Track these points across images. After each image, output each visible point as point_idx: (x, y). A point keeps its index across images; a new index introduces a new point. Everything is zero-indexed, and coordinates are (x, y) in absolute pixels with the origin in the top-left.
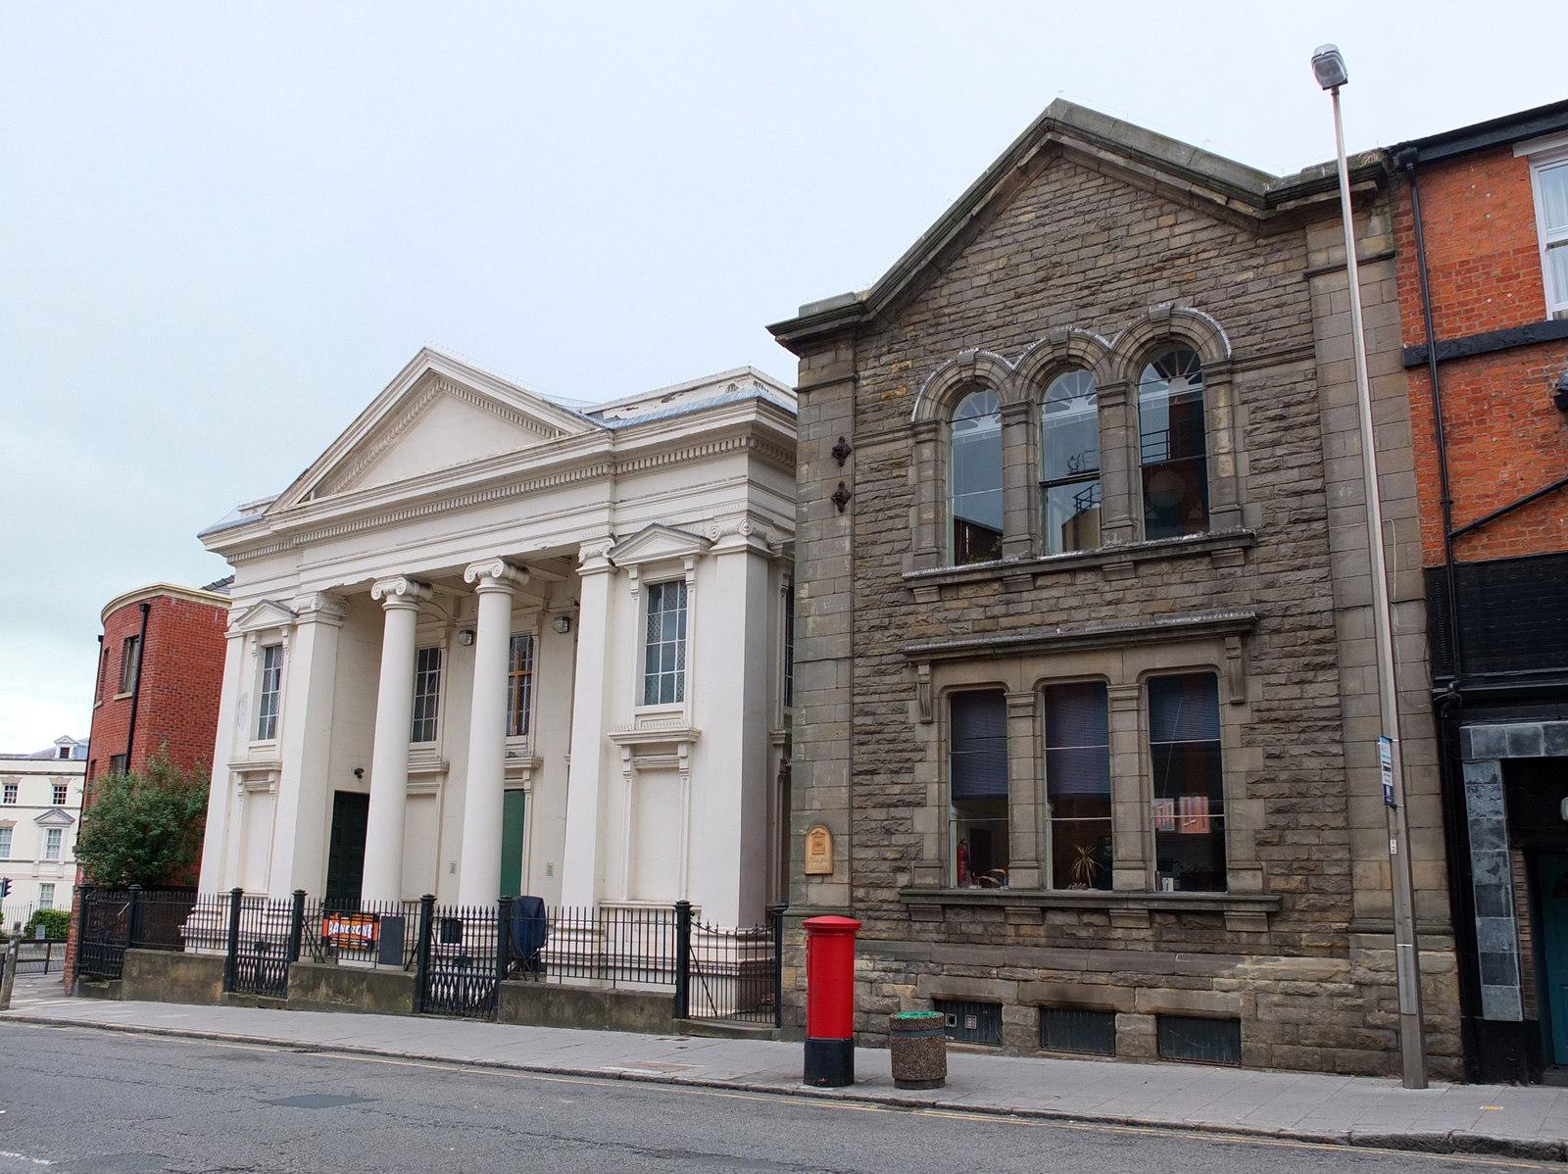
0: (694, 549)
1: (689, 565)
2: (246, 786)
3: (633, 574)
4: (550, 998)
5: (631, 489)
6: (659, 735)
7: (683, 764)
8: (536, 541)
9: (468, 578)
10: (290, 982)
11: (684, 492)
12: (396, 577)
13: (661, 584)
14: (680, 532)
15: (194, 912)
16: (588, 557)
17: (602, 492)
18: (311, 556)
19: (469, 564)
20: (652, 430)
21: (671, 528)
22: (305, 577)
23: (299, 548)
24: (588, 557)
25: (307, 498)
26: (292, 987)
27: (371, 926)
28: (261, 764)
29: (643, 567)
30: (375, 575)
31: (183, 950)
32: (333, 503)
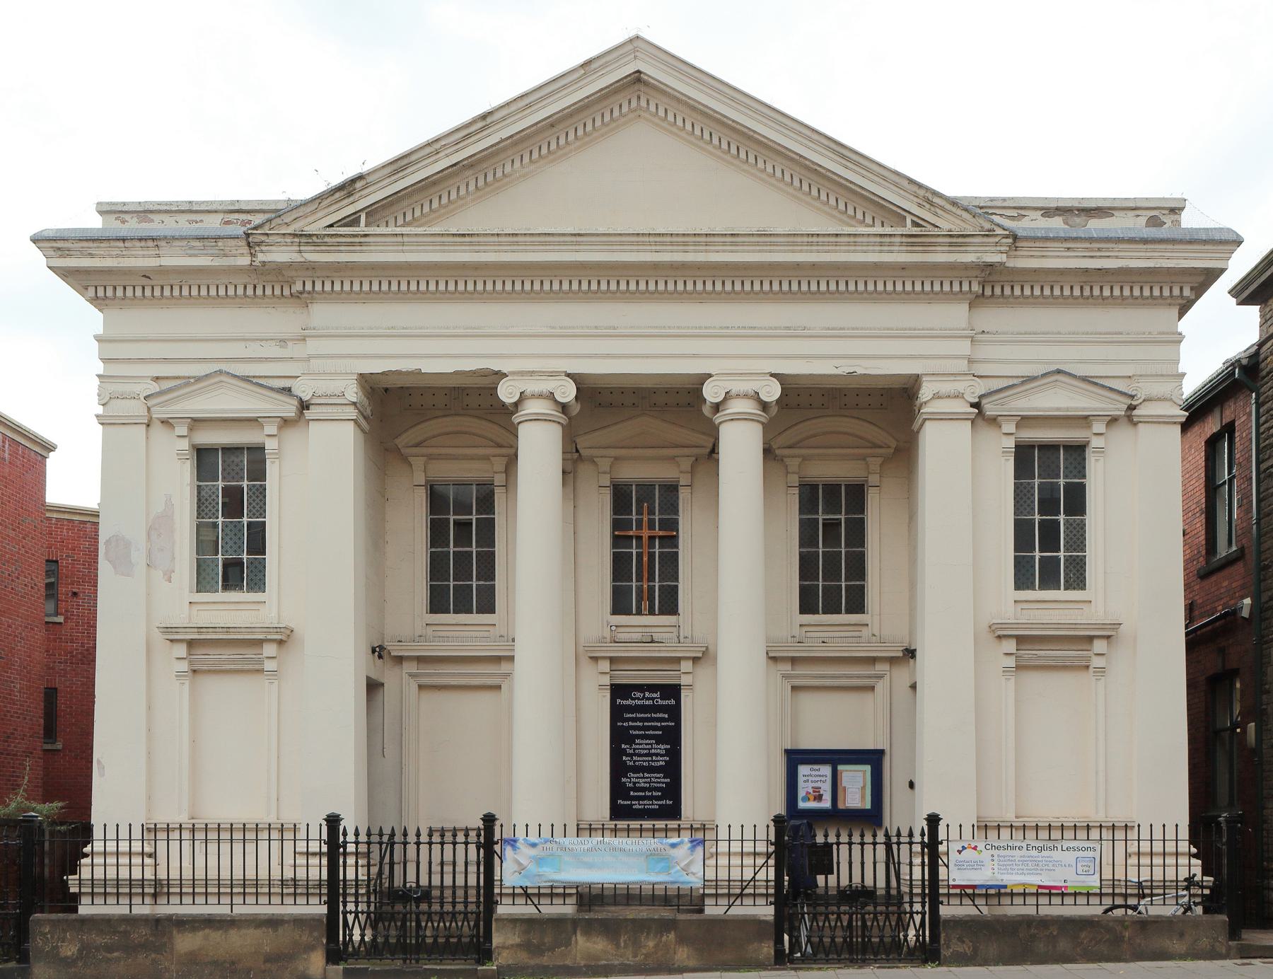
1: (1099, 427)
2: (191, 663)
5: (994, 318)
6: (1058, 626)
9: (711, 393)
11: (1084, 337)
12: (553, 374)
13: (1033, 447)
14: (1103, 387)
15: (86, 855)
16: (937, 396)
17: (956, 314)
18: (323, 314)
19: (710, 376)
21: (1085, 379)
22: (312, 346)
23: (302, 299)
24: (937, 396)
29: (1025, 421)
30: (495, 365)
31: (76, 910)
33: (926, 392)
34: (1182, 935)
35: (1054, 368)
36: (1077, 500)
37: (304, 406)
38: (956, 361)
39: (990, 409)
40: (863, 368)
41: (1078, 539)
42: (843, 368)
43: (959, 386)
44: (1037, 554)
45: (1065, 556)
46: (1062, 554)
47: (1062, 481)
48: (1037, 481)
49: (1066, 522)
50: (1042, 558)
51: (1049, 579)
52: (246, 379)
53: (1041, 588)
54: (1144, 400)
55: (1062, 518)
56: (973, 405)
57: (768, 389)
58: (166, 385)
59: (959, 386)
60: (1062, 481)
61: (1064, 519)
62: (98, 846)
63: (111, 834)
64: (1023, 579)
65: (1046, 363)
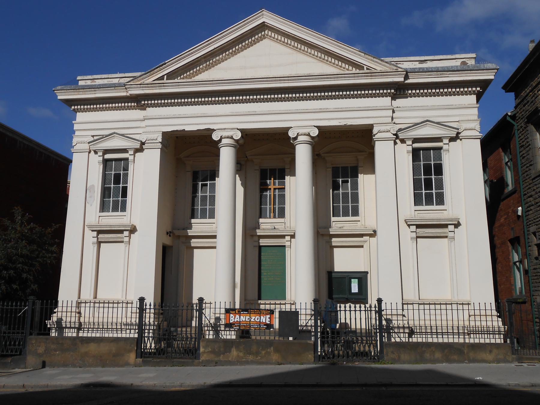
0: (452, 134)
1: (446, 141)
3: (410, 142)
4: (424, 349)
6: (433, 220)
7: (451, 235)
8: (340, 121)
10: (202, 350)
12: (232, 129)
15: (55, 313)
16: (379, 132)
17: (386, 101)
18: (151, 111)
19: (291, 127)
20: (431, 75)
21: (438, 123)
24: (379, 132)
25: (162, 78)
26: (204, 352)
27: (268, 316)
28: (119, 226)
29: (415, 140)
32: (178, 85)
33: (375, 131)
34: (491, 352)
35: (426, 119)
36: (439, 170)
37: (143, 144)
38: (386, 118)
39: (401, 136)
40: (350, 122)
41: (440, 185)
42: (342, 123)
43: (388, 128)
44: (424, 192)
45: (435, 192)
46: (434, 191)
47: (432, 163)
48: (422, 163)
49: (435, 178)
50: (426, 193)
51: (429, 201)
52: (123, 135)
53: (426, 205)
54: (464, 130)
55: (433, 177)
56: (394, 135)
57: (313, 131)
58: (96, 138)
59: (388, 128)
60: (432, 163)
61: (434, 177)
62: (60, 309)
63: (65, 305)
64: (418, 201)
65: (423, 118)
